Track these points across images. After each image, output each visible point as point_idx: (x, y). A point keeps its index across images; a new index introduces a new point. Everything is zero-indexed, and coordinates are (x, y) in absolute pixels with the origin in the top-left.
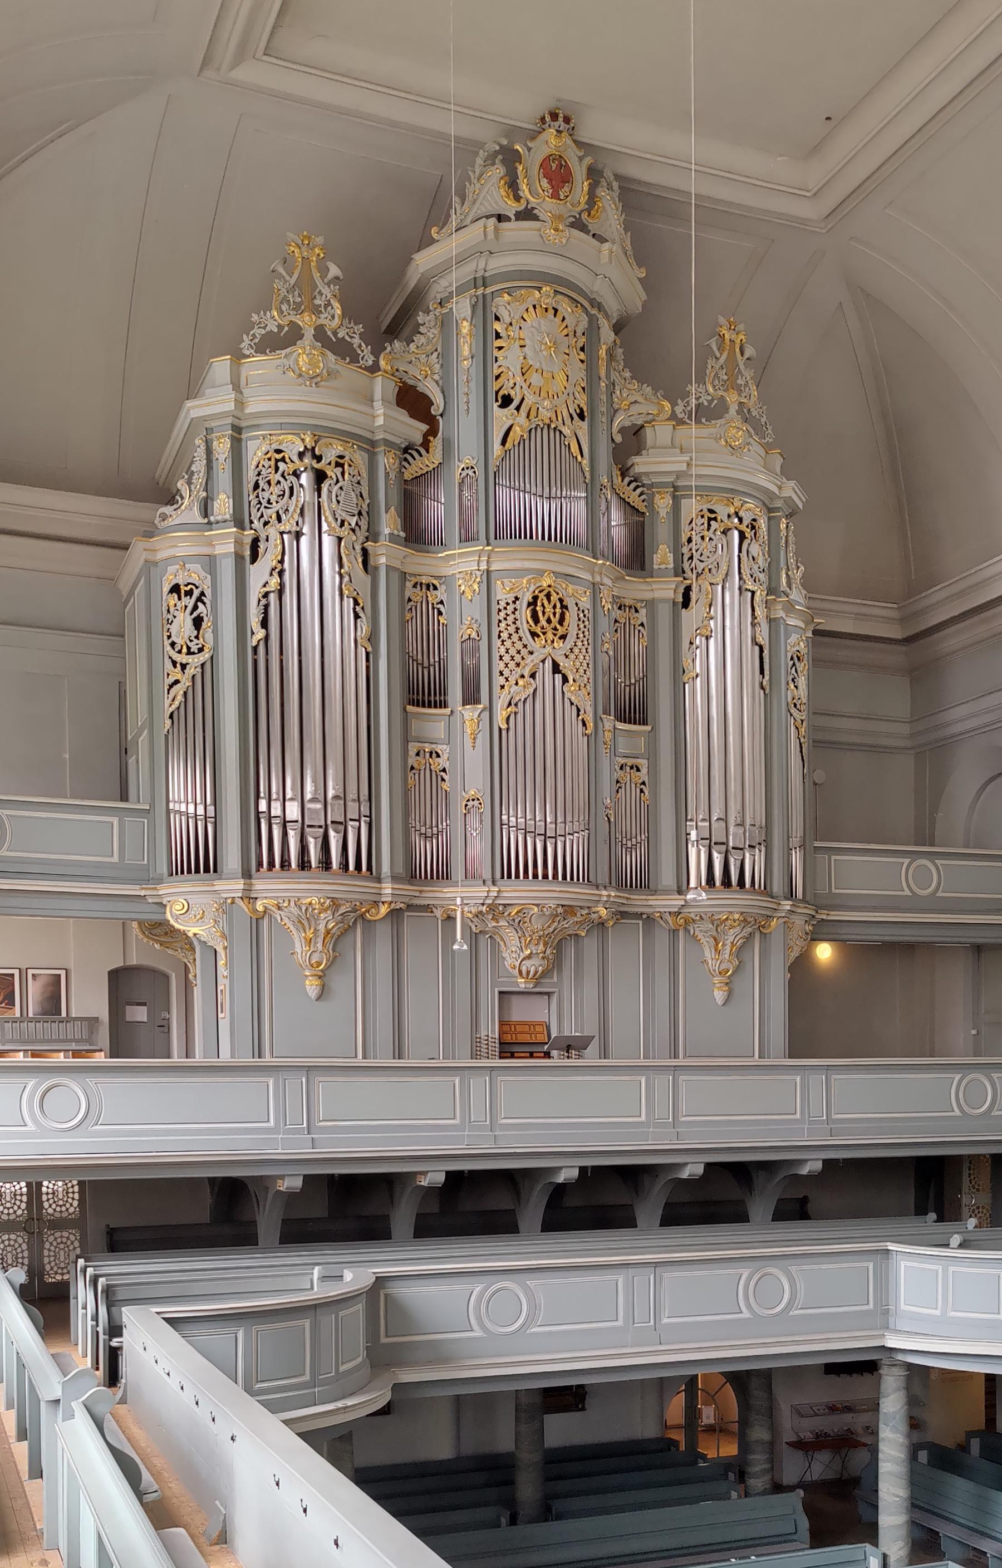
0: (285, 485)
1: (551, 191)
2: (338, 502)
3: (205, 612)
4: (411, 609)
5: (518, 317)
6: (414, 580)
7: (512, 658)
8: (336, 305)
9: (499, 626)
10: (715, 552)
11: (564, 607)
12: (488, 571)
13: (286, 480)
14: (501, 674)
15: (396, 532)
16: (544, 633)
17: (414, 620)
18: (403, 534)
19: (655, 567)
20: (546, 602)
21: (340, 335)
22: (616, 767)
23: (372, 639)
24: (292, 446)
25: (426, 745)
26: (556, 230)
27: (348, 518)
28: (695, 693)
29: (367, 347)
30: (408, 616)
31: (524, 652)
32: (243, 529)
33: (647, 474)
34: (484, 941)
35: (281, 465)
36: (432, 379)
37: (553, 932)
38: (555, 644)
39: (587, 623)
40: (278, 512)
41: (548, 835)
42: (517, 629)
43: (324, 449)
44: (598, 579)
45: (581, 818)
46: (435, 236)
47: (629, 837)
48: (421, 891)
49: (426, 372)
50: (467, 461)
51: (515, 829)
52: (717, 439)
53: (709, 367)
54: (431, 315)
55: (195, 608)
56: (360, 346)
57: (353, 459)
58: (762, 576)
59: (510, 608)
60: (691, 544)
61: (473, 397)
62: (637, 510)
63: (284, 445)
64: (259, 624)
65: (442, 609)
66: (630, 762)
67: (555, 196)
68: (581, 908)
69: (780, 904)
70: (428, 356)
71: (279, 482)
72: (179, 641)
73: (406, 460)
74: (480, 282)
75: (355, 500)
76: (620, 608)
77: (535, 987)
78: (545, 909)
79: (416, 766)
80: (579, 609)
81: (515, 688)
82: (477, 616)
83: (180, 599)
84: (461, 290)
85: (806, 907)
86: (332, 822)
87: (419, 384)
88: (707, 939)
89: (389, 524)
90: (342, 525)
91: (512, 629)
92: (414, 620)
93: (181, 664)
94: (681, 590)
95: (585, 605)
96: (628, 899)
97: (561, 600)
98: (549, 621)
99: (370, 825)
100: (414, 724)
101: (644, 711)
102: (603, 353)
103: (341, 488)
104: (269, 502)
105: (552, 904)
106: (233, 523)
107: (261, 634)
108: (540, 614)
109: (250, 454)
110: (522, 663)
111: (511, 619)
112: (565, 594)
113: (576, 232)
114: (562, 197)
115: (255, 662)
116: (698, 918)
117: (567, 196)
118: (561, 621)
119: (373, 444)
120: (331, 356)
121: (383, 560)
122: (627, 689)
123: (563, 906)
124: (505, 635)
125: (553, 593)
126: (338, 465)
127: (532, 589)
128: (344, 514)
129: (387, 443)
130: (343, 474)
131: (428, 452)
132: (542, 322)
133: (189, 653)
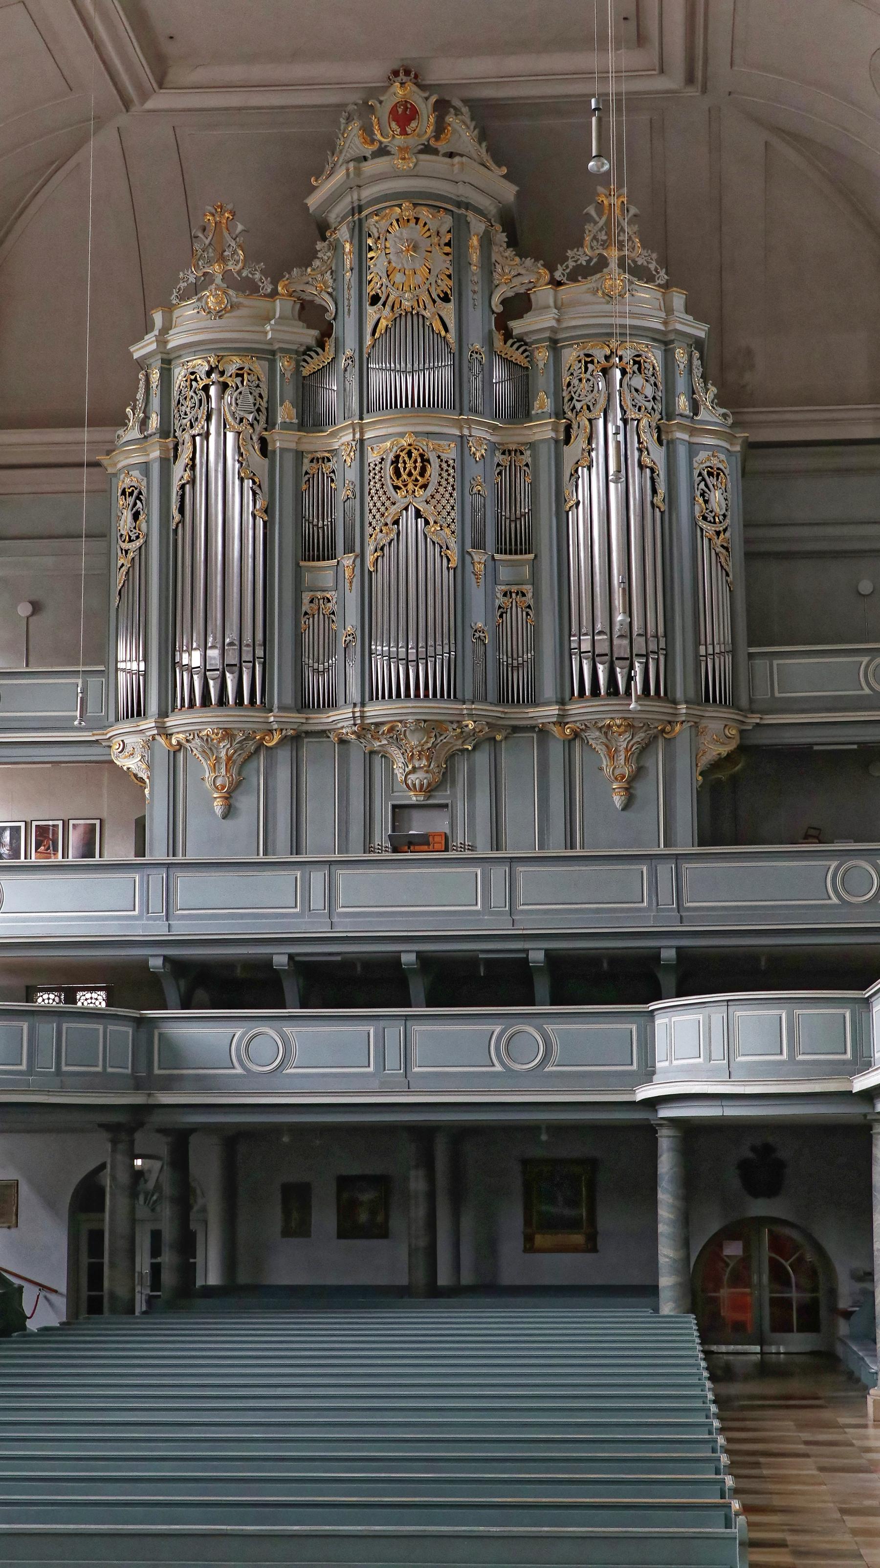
0: (196, 398)
1: (399, 130)
2: (237, 404)
3: (141, 507)
4: (309, 480)
5: (383, 231)
6: (310, 456)
7: (378, 509)
8: (241, 252)
9: (369, 484)
10: (592, 391)
11: (425, 461)
12: (362, 441)
13: (197, 395)
14: (370, 524)
15: (287, 420)
16: (405, 486)
17: (311, 489)
18: (295, 421)
19: (533, 412)
20: (407, 459)
21: (244, 275)
22: (499, 596)
23: (269, 511)
24: (202, 367)
25: (319, 593)
26: (404, 159)
27: (246, 415)
28: (578, 519)
29: (266, 279)
30: (304, 487)
31: (388, 503)
32: (168, 437)
33: (526, 333)
34: (377, 759)
35: (194, 383)
36: (326, 291)
37: (434, 745)
38: (416, 493)
39: (451, 471)
40: (191, 421)
41: (409, 659)
42: (383, 485)
43: (226, 366)
44: (466, 432)
45: (446, 641)
46: (314, 183)
47: (515, 656)
48: (307, 719)
49: (321, 287)
50: (348, 353)
51: (395, 660)
52: (595, 292)
53: (587, 232)
54: (327, 242)
55: (135, 504)
56: (261, 279)
57: (252, 368)
58: (650, 405)
59: (377, 468)
60: (569, 389)
61: (352, 302)
62: (521, 366)
63: (197, 367)
64: (177, 511)
65: (334, 477)
66: (514, 588)
67: (404, 132)
68: (452, 722)
69: (677, 709)
70: (322, 275)
71: (192, 397)
72: (124, 532)
73: (305, 361)
74: (356, 210)
75: (251, 399)
76: (503, 453)
77: (429, 798)
78: (408, 725)
79: (309, 611)
80: (442, 461)
81: (380, 535)
82: (353, 480)
83: (125, 499)
84: (344, 218)
85: (717, 711)
86: (227, 665)
87: (316, 298)
88: (599, 747)
89: (285, 413)
90: (241, 420)
91: (378, 486)
92: (311, 489)
93: (125, 550)
94: (562, 429)
95: (448, 456)
96: (503, 712)
97: (422, 456)
98: (410, 474)
99: (264, 665)
100: (307, 577)
101: (529, 542)
102: (475, 241)
103: (240, 393)
104: (186, 414)
105: (411, 719)
106: (158, 435)
107: (177, 517)
108: (402, 470)
109: (176, 378)
110: (386, 514)
111: (377, 477)
112: (426, 449)
113: (422, 157)
114: (408, 130)
115: (176, 541)
116: (583, 727)
117: (414, 130)
118: (422, 474)
119: (273, 353)
120: (231, 292)
121: (278, 444)
122: (513, 525)
123: (425, 721)
124: (373, 491)
125: (413, 451)
126: (237, 375)
127: (394, 450)
128: (242, 413)
129: (282, 350)
130: (242, 382)
131: (324, 350)
132: (404, 231)
133: (130, 541)
